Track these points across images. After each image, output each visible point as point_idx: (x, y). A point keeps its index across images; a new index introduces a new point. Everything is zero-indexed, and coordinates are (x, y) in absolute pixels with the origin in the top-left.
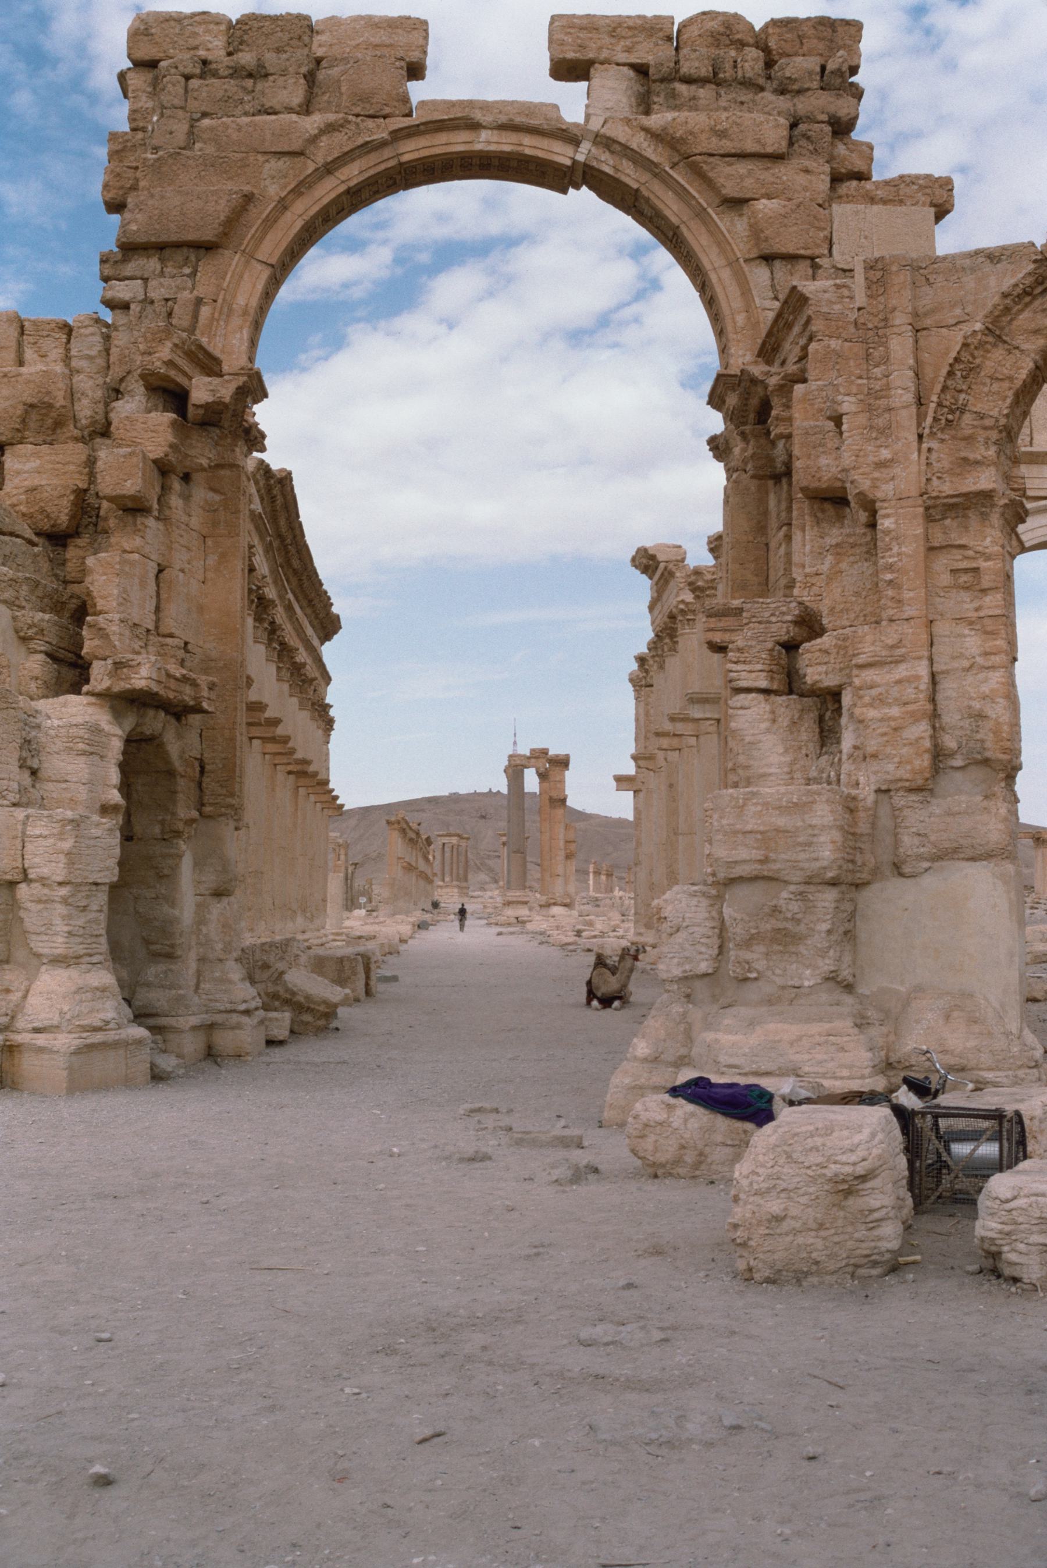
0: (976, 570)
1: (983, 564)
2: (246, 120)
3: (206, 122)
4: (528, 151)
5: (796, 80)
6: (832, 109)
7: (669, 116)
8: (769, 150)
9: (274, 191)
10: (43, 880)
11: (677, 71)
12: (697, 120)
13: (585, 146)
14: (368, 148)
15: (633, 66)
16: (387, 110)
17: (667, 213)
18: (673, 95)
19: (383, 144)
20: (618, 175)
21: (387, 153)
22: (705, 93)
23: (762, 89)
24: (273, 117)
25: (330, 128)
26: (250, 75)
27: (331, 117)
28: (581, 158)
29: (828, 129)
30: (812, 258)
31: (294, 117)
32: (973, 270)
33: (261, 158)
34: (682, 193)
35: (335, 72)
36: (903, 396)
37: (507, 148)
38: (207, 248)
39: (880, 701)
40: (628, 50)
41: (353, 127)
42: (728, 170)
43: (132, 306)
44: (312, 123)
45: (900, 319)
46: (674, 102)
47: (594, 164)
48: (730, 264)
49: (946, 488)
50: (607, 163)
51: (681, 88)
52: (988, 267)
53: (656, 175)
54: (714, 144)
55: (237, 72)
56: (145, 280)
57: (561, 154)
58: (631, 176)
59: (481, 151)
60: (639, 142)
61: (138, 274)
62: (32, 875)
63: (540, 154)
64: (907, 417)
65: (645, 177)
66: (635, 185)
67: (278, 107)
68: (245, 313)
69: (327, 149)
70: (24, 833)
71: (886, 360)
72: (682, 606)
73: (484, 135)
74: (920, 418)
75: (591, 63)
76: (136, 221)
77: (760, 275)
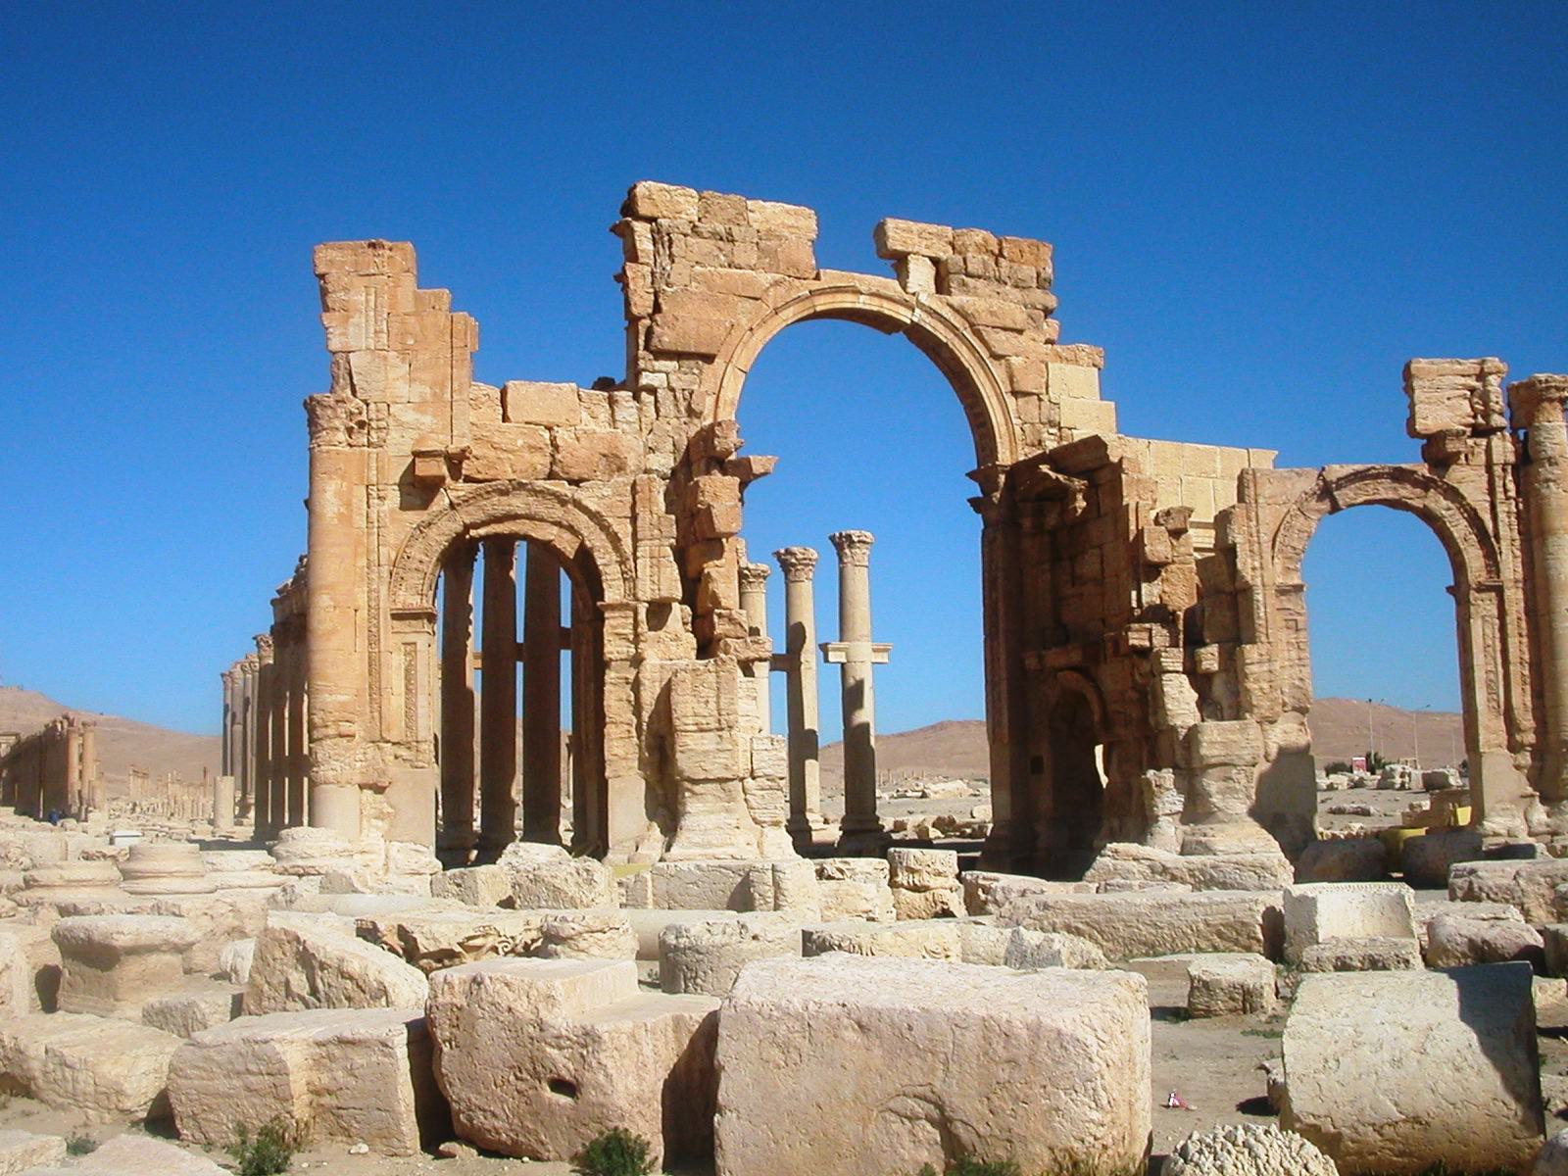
0: (1296, 620)
1: (1298, 618)
2: (720, 269)
4: (886, 312)
5: (1024, 281)
6: (1042, 301)
7: (965, 298)
8: (1018, 327)
9: (744, 322)
11: (966, 269)
14: (799, 300)
15: (931, 259)
16: (807, 275)
17: (962, 359)
18: (964, 284)
19: (807, 298)
20: (936, 333)
21: (808, 304)
22: (980, 283)
23: (1006, 284)
24: (741, 271)
25: (777, 283)
26: (721, 239)
27: (778, 277)
28: (915, 320)
29: (1043, 314)
32: (1290, 479)
33: (735, 298)
34: (972, 348)
35: (773, 243)
37: (875, 309)
38: (709, 359)
39: (1257, 681)
40: (927, 247)
41: (787, 283)
42: (993, 335)
44: (765, 278)
47: (923, 324)
48: (997, 395)
49: (1279, 580)
50: (930, 324)
51: (968, 280)
52: (1296, 478)
53: (956, 335)
54: (990, 320)
55: (716, 236)
56: (667, 374)
57: (904, 315)
58: (943, 334)
59: (860, 309)
61: (663, 369)
62: (758, 773)
65: (951, 336)
66: (945, 340)
67: (743, 265)
68: (732, 403)
69: (775, 297)
70: (752, 749)
72: (746, 572)
75: (909, 253)
76: (668, 336)
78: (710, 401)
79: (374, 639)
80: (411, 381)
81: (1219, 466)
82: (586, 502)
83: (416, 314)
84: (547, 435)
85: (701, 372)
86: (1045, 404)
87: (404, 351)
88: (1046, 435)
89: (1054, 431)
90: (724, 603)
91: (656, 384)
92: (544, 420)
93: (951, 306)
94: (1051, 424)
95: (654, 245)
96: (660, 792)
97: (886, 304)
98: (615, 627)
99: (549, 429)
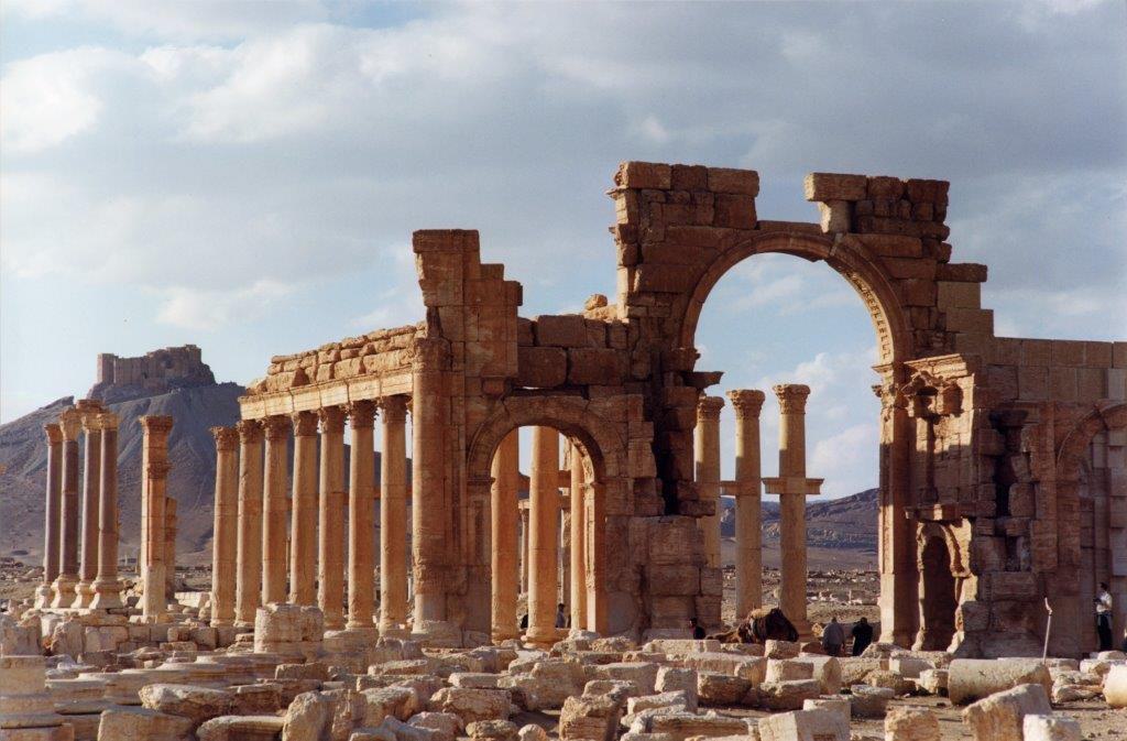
3: (671, 228)
5: (922, 216)
10: (711, 595)
12: (886, 240)
13: (834, 249)
22: (886, 223)
25: (726, 236)
30: (929, 307)
31: (711, 229)
36: (1051, 448)
43: (642, 320)
44: (720, 232)
45: (1051, 423)
46: (871, 230)
51: (875, 221)
56: (647, 307)
60: (857, 247)
62: (704, 592)
63: (814, 251)
64: (1052, 455)
71: (1046, 435)
73: (792, 241)
74: (1057, 455)
77: (908, 313)
78: (677, 325)
79: (456, 499)
80: (479, 327)
81: (1085, 358)
82: (596, 413)
83: (482, 280)
84: (564, 354)
85: (671, 305)
86: (934, 317)
87: (475, 306)
88: (934, 338)
89: (941, 335)
90: (684, 476)
91: (639, 314)
92: (562, 344)
93: (861, 242)
94: (938, 328)
95: (639, 208)
96: (640, 602)
97: (809, 244)
98: (613, 495)
99: (566, 349)
